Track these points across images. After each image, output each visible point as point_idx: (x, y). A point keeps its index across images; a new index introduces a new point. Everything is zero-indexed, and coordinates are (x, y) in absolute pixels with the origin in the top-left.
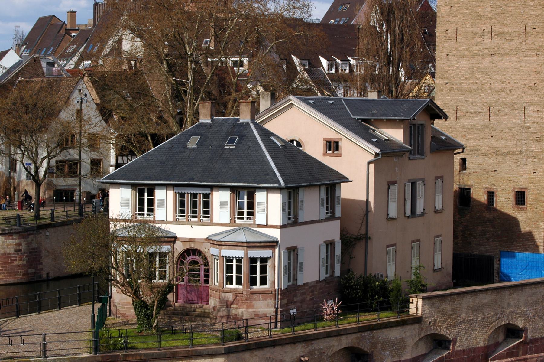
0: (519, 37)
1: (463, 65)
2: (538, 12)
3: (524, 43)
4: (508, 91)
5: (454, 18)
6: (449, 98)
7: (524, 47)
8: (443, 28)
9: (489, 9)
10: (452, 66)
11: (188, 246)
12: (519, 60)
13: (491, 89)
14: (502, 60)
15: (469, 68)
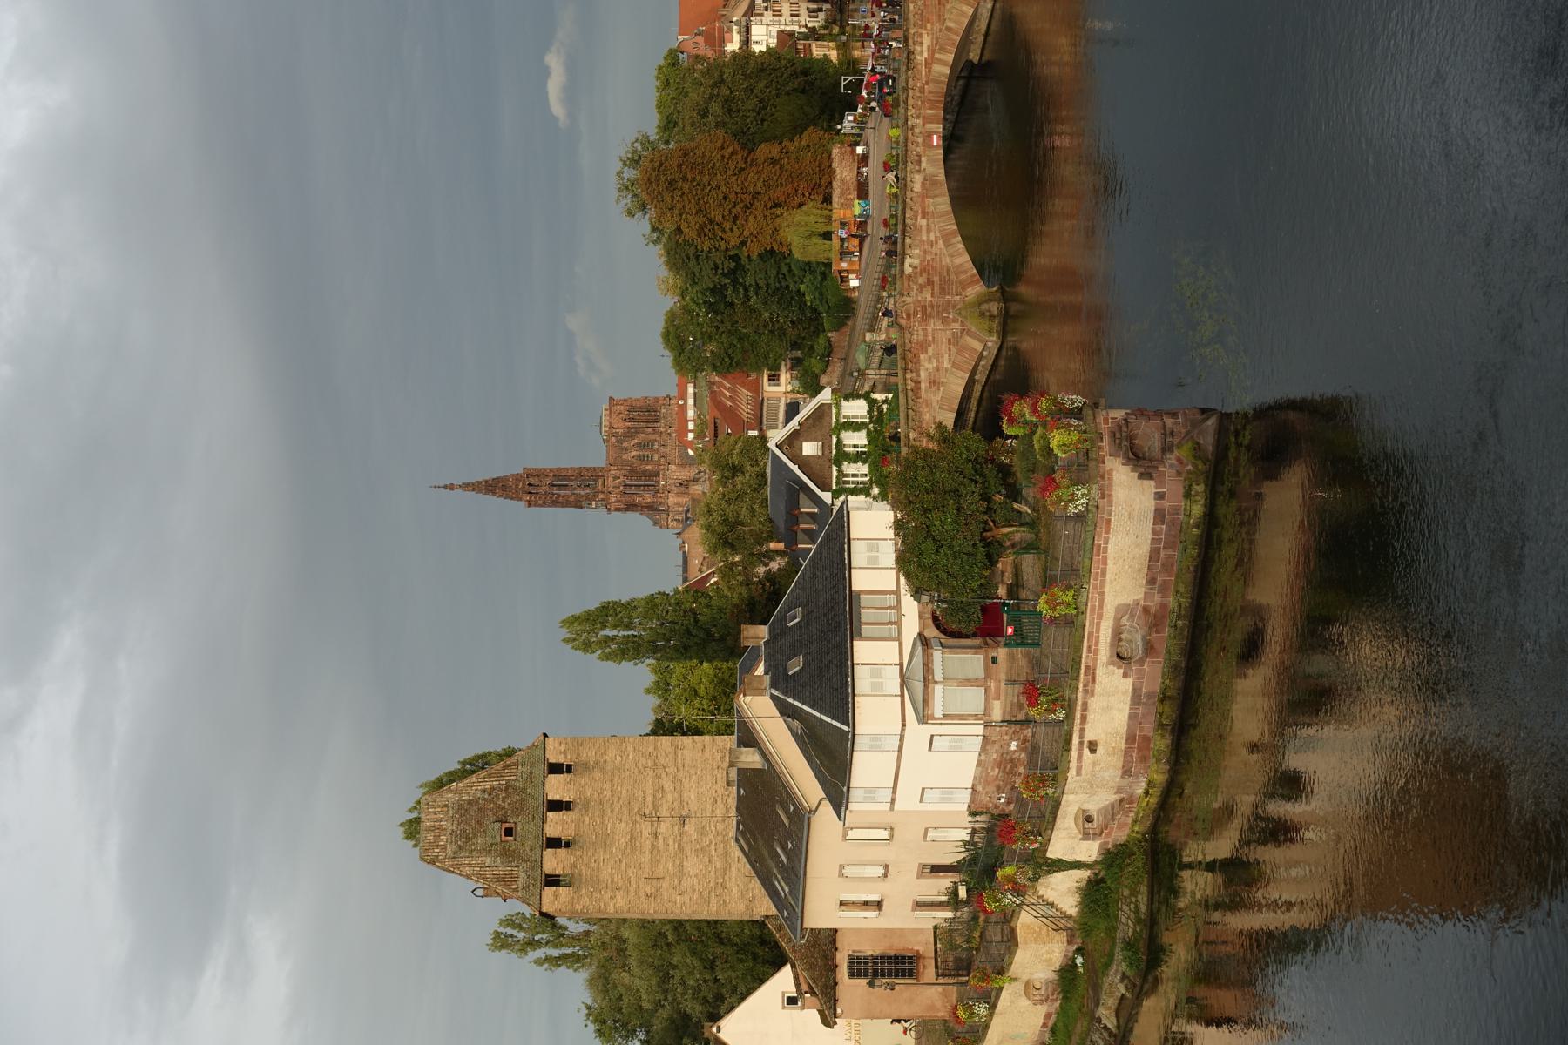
0: (660, 777)
1: (693, 865)
2: (630, 749)
3: (667, 770)
4: (727, 793)
5: (632, 883)
6: (735, 890)
7: (671, 770)
8: (644, 901)
9: (623, 825)
10: (693, 885)
11: (930, 622)
12: (688, 779)
13: (724, 821)
14: (688, 803)
15: (697, 856)
